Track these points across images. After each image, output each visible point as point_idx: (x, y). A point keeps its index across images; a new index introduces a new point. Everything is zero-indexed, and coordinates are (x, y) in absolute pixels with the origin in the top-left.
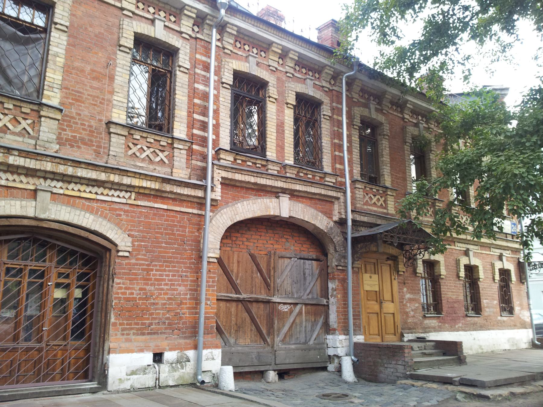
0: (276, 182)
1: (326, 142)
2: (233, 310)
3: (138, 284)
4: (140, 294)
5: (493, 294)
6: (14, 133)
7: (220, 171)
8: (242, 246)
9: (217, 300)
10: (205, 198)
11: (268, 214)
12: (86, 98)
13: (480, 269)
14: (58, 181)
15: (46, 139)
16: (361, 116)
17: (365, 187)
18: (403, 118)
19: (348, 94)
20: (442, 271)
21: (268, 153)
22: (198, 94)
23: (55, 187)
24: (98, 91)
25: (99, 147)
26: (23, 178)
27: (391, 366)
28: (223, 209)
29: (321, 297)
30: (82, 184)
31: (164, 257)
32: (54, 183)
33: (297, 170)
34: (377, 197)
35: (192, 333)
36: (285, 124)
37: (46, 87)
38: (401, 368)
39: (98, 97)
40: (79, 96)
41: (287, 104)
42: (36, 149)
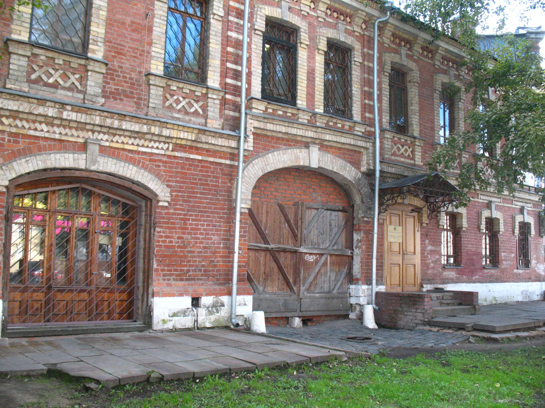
0: (307, 132)
1: (356, 90)
2: (262, 259)
3: (176, 232)
4: (178, 242)
5: (512, 247)
6: (64, 88)
7: (252, 121)
8: (270, 197)
9: (248, 249)
10: (238, 148)
11: (297, 164)
12: (127, 51)
13: (500, 222)
14: (104, 133)
15: (92, 93)
16: (392, 62)
17: (394, 137)
18: (434, 65)
19: (379, 39)
20: (464, 223)
21: (298, 102)
22: (231, 42)
23: (102, 140)
24: (138, 43)
25: (141, 99)
26: (74, 132)
27: (411, 314)
28: (255, 159)
29: (346, 248)
30: (125, 136)
31: (198, 207)
32: (101, 136)
33: (327, 119)
34: (405, 147)
35: (225, 279)
36: (316, 71)
37: (91, 41)
38: (420, 316)
39: (137, 49)
40: (121, 49)
41: (319, 50)
42: (84, 103)
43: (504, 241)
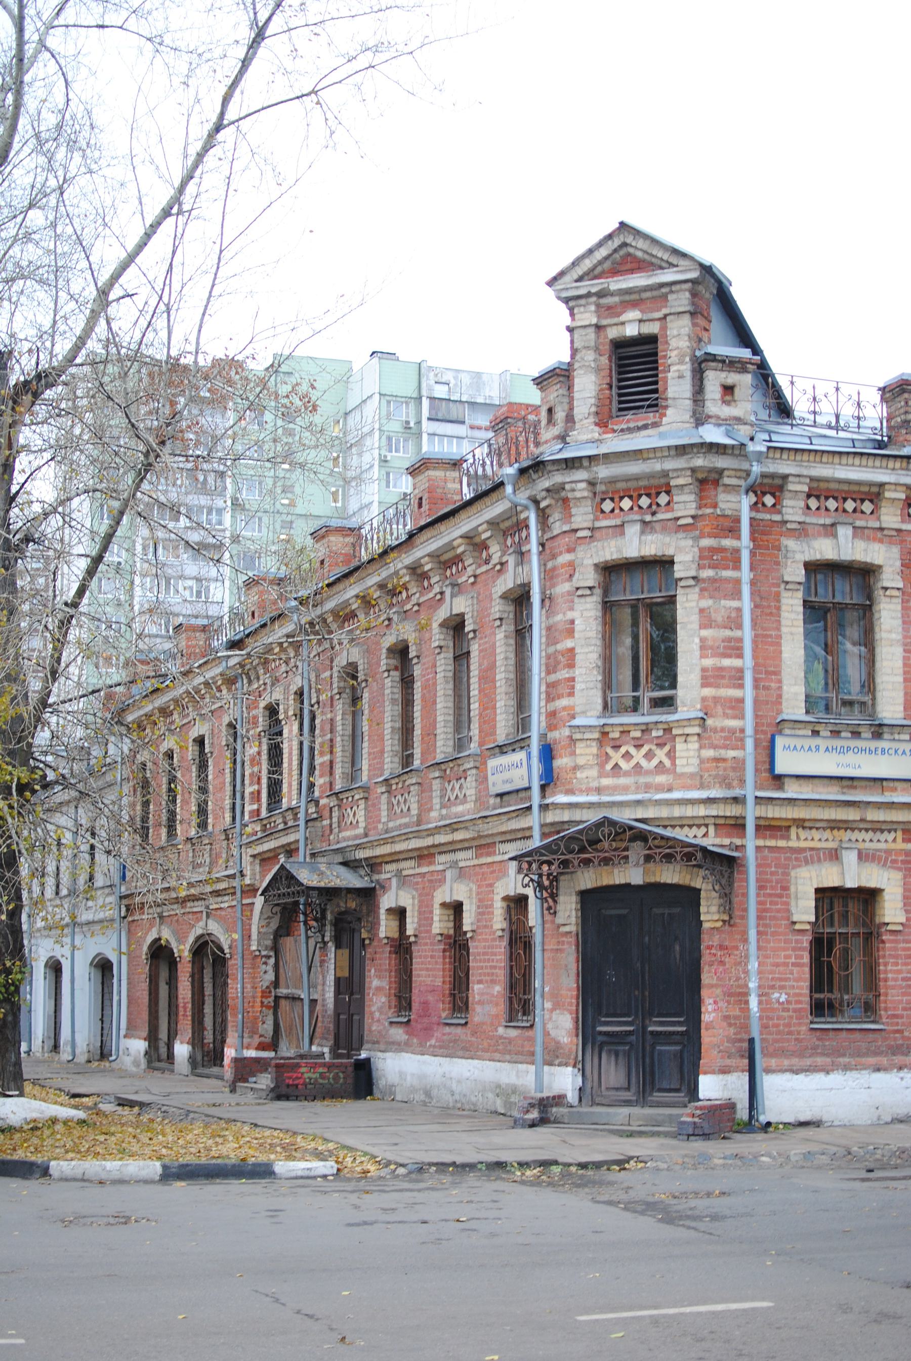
43: (479, 954)
